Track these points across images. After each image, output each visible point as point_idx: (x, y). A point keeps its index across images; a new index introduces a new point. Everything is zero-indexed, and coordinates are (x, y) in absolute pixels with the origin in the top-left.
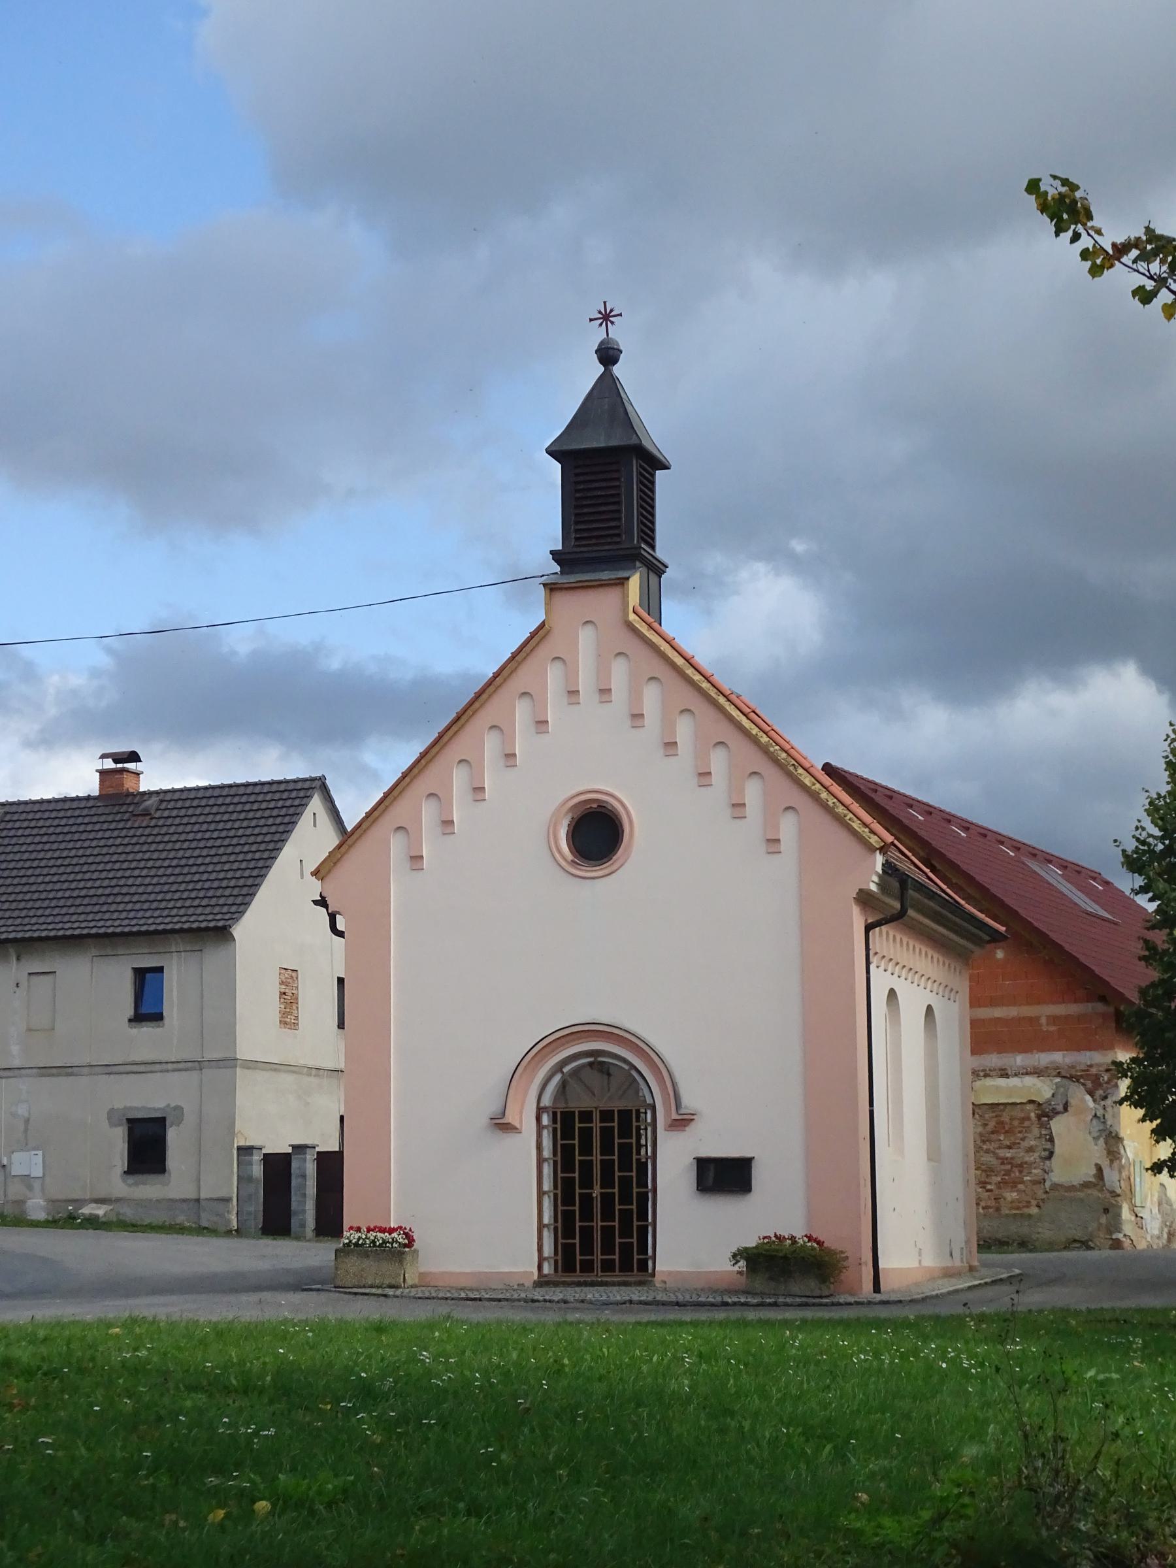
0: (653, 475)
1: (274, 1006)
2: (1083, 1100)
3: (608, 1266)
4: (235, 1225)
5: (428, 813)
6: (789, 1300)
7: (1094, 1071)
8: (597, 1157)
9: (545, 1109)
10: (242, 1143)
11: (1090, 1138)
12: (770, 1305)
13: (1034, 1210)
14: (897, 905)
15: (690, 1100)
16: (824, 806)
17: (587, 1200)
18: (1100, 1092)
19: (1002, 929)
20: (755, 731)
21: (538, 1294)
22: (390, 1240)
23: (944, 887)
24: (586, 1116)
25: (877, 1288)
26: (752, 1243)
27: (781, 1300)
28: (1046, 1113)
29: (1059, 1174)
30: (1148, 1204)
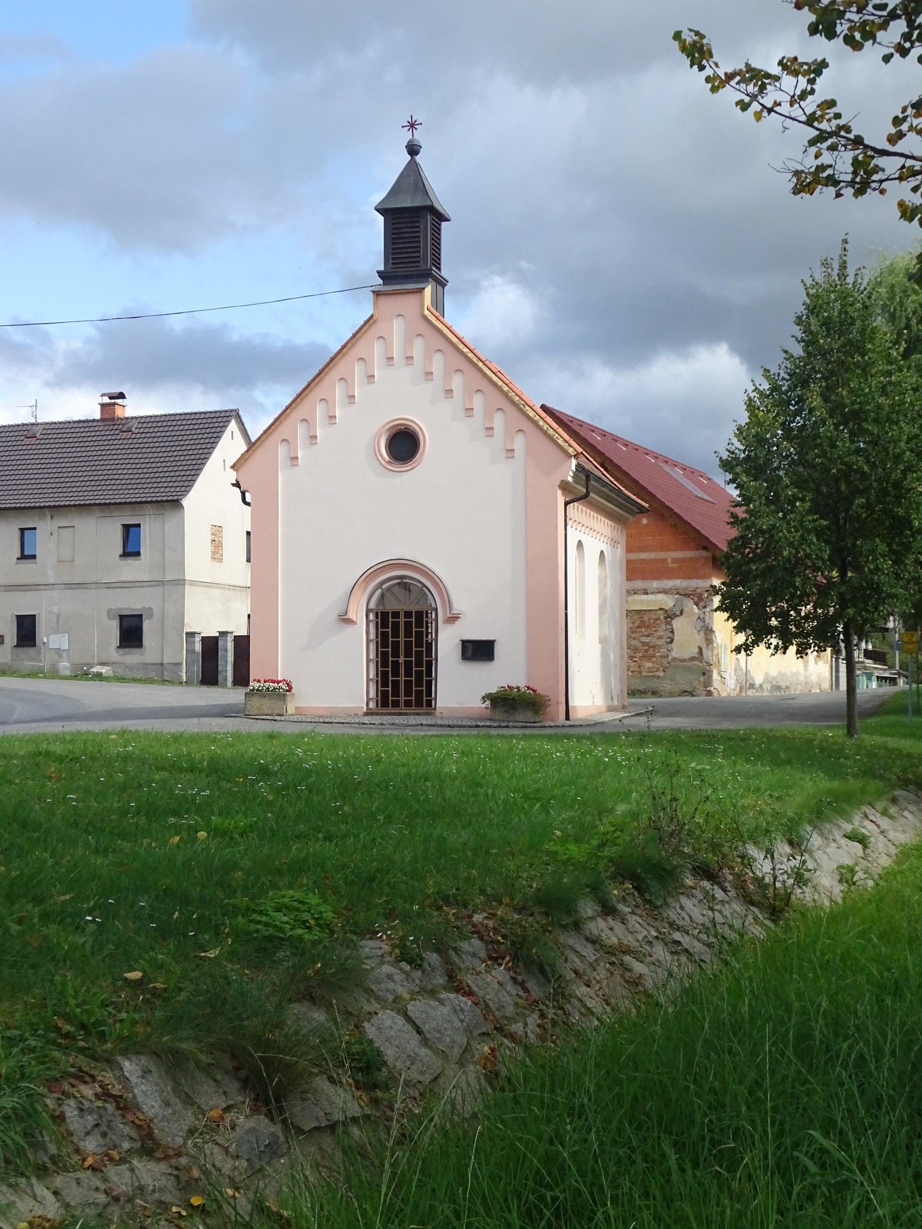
0: (440, 225)
1: (208, 547)
2: (692, 609)
3: (408, 704)
4: (185, 680)
5: (301, 431)
6: (516, 724)
7: (699, 591)
8: (402, 639)
9: (371, 610)
10: (189, 630)
11: (695, 631)
12: (504, 727)
13: (661, 674)
14: (585, 491)
16: (541, 429)
17: (396, 665)
18: (702, 604)
19: (647, 505)
20: (500, 383)
21: (367, 720)
23: (612, 480)
24: (396, 614)
25: (567, 718)
26: (494, 691)
27: (511, 724)
28: (670, 616)
29: (676, 652)
30: (729, 670)
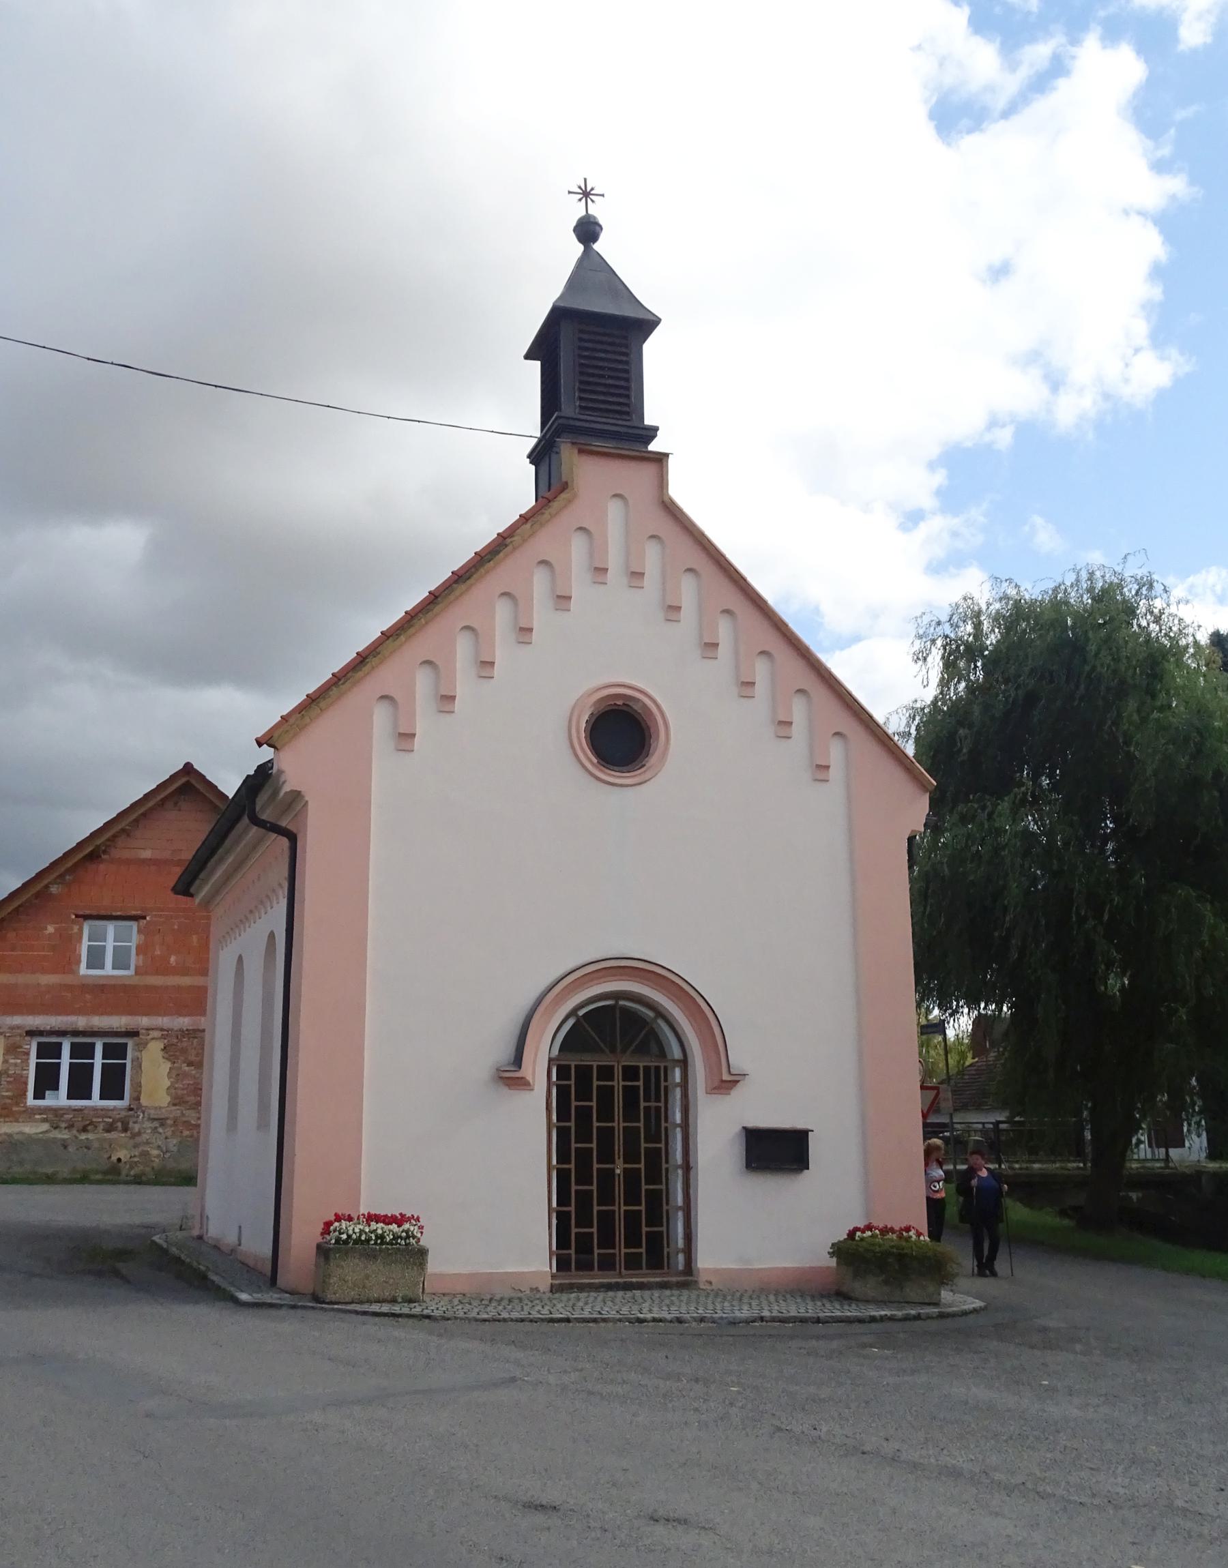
15: (740, 1056)
22: (404, 1234)
